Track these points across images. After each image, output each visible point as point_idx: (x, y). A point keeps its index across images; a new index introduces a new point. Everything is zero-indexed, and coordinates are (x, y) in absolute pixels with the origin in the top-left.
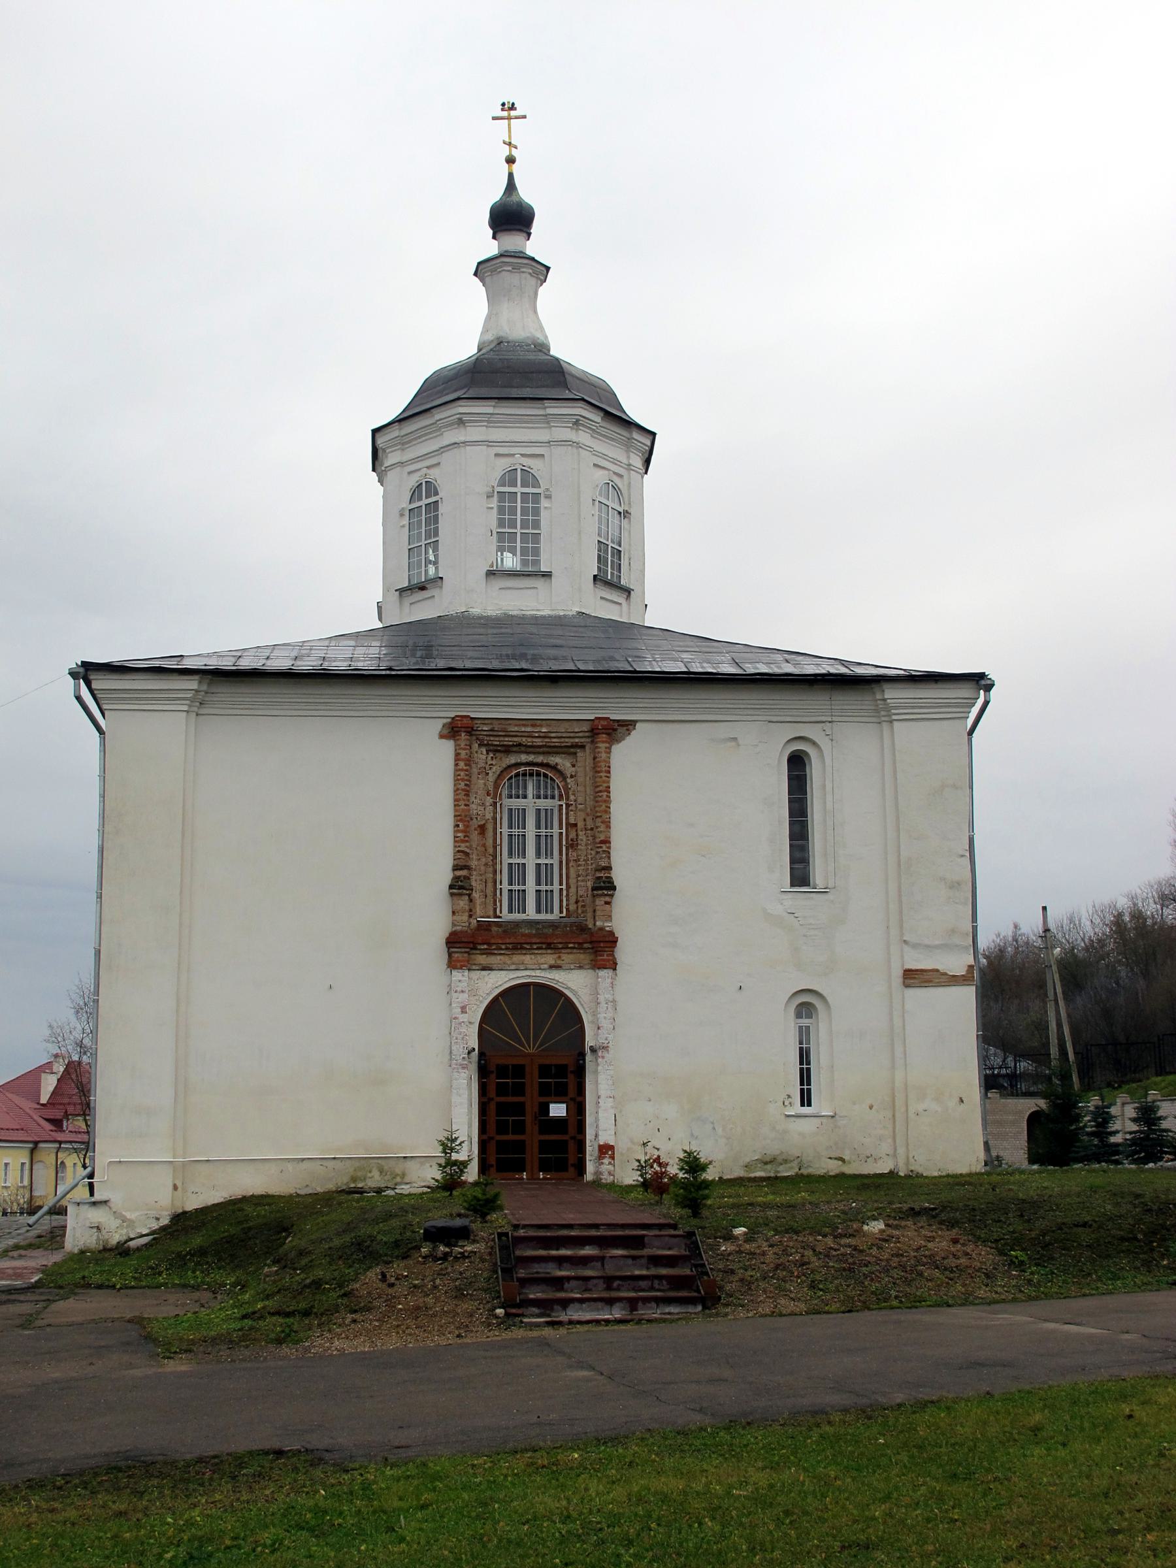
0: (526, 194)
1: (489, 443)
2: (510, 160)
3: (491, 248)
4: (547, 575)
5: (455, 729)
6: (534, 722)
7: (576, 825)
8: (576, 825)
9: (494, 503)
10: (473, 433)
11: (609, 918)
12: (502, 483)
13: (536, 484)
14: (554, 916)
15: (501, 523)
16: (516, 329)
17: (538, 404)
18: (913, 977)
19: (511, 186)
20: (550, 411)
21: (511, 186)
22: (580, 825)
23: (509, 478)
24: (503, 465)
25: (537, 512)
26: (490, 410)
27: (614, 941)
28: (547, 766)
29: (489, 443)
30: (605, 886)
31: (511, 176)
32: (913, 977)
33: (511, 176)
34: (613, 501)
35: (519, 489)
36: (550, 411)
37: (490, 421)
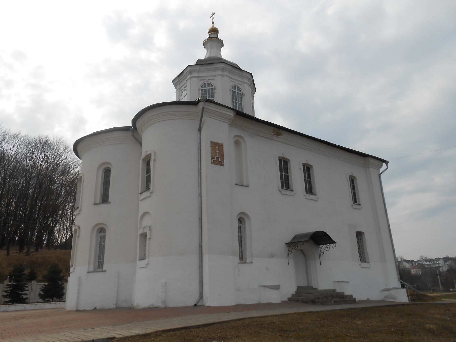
0: (216, 26)
1: (198, 77)
9: (200, 92)
10: (195, 75)
12: (202, 86)
13: (212, 86)
16: (213, 55)
17: (211, 65)
20: (214, 66)
24: (202, 82)
25: (212, 93)
26: (198, 68)
29: (198, 77)
34: (238, 90)
36: (214, 66)
37: (199, 71)
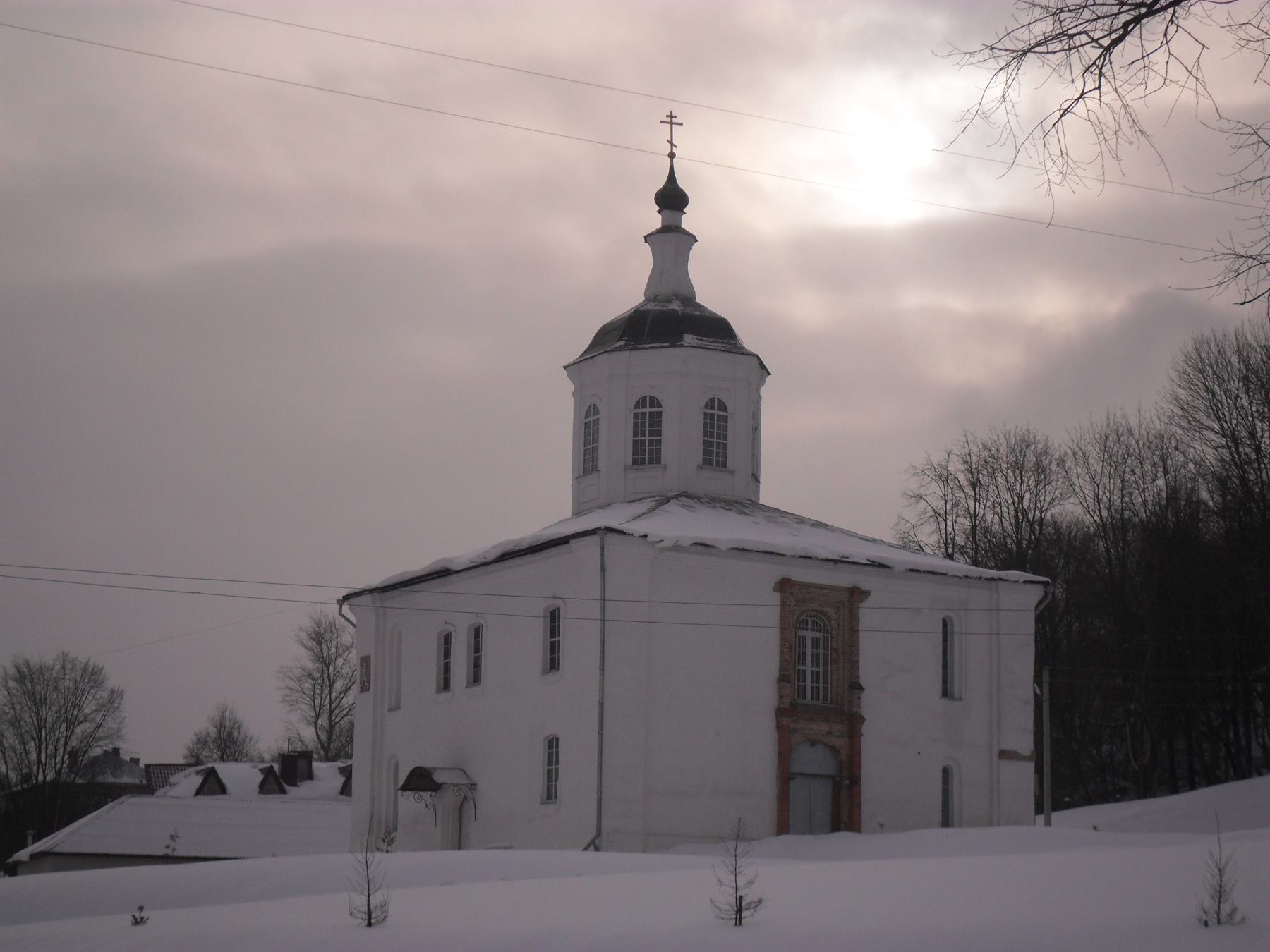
0: (682, 183)
2: (672, 155)
3: (655, 220)
4: (732, 472)
5: (784, 585)
6: (821, 587)
7: (836, 650)
8: (836, 650)
11: (859, 707)
13: (725, 410)
14: (818, 703)
15: (705, 435)
18: (1004, 755)
19: (672, 177)
21: (672, 177)
22: (840, 650)
23: (710, 404)
27: (861, 720)
28: (822, 612)
30: (856, 687)
31: (672, 168)
32: (1004, 755)
33: (672, 168)
35: (716, 412)
